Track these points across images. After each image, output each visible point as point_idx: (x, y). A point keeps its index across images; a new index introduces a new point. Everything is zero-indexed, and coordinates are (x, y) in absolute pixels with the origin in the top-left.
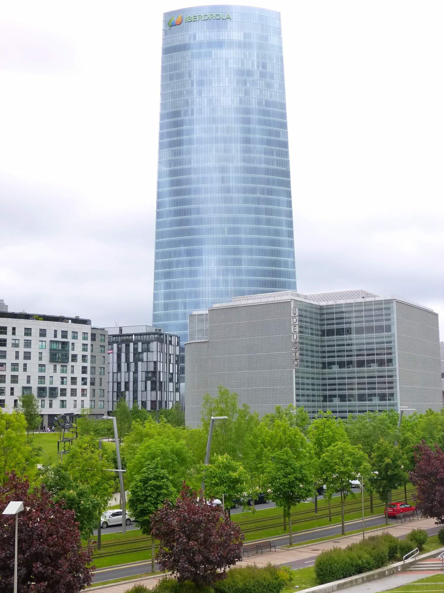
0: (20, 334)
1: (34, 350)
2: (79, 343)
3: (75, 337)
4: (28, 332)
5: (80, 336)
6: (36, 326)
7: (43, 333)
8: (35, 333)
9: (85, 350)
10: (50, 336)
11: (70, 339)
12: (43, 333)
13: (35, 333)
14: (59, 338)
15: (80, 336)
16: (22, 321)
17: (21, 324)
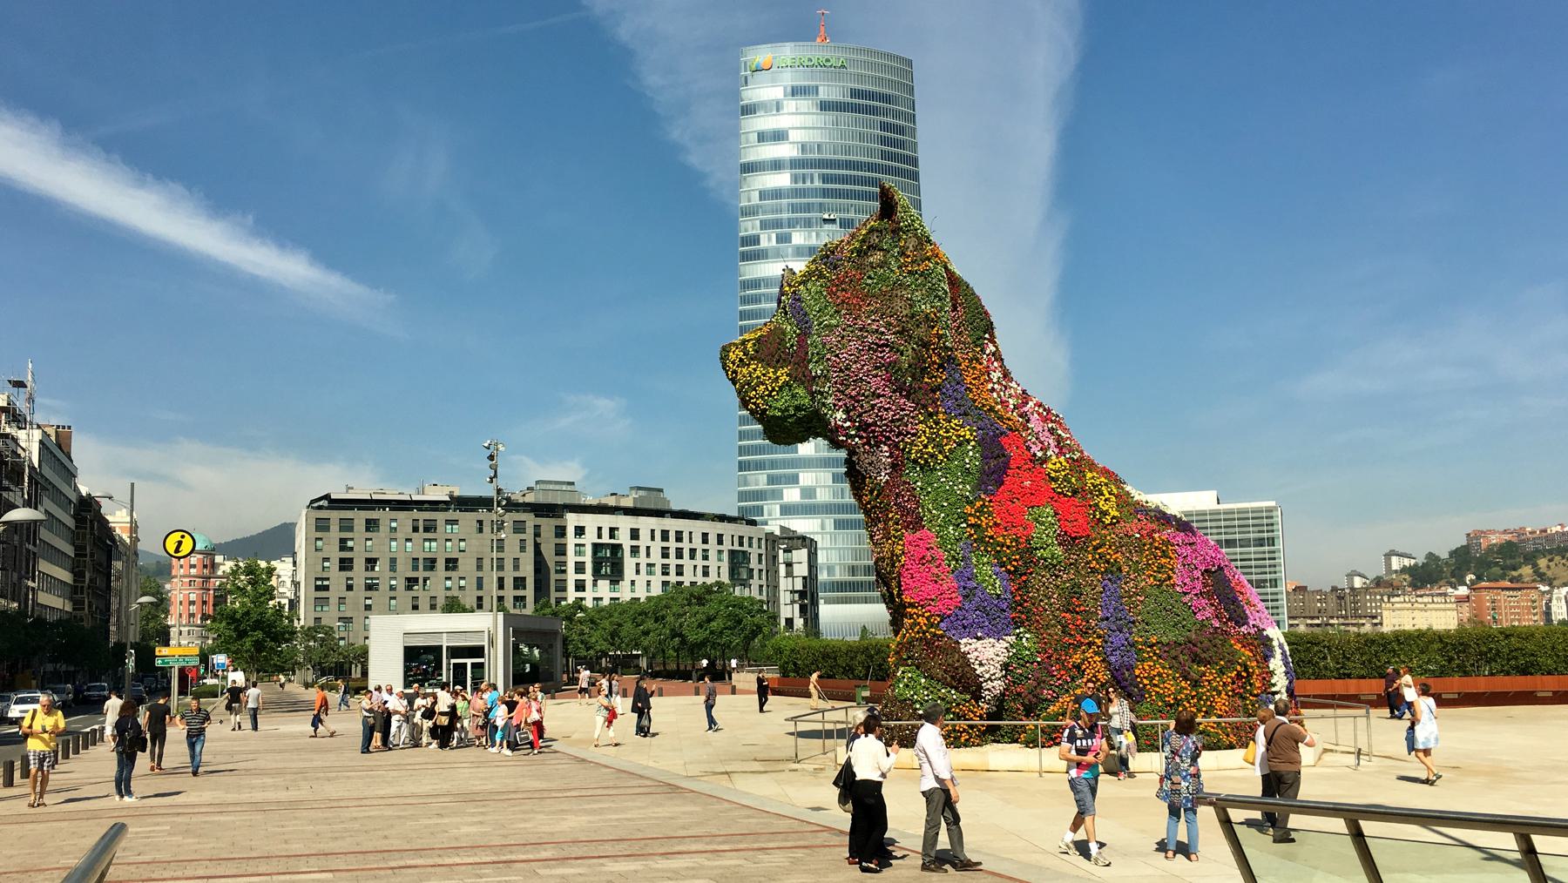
0: (697, 539)
1: (713, 563)
2: (754, 553)
3: (750, 545)
4: (705, 541)
5: (755, 544)
6: (713, 529)
7: (720, 540)
8: (712, 539)
9: (760, 562)
10: (727, 546)
11: (746, 547)
12: (720, 540)
13: (712, 539)
14: (736, 547)
15: (755, 544)
16: (698, 523)
17: (698, 527)
